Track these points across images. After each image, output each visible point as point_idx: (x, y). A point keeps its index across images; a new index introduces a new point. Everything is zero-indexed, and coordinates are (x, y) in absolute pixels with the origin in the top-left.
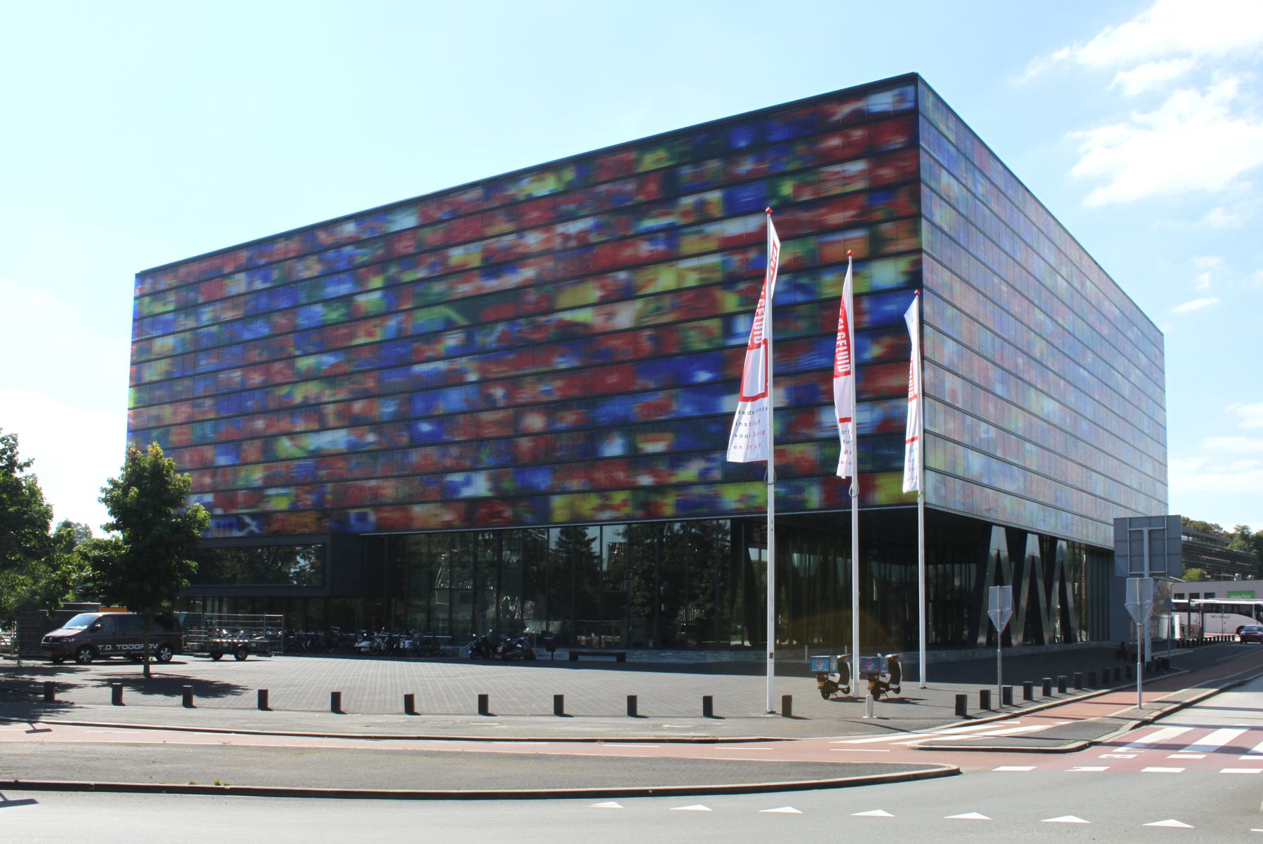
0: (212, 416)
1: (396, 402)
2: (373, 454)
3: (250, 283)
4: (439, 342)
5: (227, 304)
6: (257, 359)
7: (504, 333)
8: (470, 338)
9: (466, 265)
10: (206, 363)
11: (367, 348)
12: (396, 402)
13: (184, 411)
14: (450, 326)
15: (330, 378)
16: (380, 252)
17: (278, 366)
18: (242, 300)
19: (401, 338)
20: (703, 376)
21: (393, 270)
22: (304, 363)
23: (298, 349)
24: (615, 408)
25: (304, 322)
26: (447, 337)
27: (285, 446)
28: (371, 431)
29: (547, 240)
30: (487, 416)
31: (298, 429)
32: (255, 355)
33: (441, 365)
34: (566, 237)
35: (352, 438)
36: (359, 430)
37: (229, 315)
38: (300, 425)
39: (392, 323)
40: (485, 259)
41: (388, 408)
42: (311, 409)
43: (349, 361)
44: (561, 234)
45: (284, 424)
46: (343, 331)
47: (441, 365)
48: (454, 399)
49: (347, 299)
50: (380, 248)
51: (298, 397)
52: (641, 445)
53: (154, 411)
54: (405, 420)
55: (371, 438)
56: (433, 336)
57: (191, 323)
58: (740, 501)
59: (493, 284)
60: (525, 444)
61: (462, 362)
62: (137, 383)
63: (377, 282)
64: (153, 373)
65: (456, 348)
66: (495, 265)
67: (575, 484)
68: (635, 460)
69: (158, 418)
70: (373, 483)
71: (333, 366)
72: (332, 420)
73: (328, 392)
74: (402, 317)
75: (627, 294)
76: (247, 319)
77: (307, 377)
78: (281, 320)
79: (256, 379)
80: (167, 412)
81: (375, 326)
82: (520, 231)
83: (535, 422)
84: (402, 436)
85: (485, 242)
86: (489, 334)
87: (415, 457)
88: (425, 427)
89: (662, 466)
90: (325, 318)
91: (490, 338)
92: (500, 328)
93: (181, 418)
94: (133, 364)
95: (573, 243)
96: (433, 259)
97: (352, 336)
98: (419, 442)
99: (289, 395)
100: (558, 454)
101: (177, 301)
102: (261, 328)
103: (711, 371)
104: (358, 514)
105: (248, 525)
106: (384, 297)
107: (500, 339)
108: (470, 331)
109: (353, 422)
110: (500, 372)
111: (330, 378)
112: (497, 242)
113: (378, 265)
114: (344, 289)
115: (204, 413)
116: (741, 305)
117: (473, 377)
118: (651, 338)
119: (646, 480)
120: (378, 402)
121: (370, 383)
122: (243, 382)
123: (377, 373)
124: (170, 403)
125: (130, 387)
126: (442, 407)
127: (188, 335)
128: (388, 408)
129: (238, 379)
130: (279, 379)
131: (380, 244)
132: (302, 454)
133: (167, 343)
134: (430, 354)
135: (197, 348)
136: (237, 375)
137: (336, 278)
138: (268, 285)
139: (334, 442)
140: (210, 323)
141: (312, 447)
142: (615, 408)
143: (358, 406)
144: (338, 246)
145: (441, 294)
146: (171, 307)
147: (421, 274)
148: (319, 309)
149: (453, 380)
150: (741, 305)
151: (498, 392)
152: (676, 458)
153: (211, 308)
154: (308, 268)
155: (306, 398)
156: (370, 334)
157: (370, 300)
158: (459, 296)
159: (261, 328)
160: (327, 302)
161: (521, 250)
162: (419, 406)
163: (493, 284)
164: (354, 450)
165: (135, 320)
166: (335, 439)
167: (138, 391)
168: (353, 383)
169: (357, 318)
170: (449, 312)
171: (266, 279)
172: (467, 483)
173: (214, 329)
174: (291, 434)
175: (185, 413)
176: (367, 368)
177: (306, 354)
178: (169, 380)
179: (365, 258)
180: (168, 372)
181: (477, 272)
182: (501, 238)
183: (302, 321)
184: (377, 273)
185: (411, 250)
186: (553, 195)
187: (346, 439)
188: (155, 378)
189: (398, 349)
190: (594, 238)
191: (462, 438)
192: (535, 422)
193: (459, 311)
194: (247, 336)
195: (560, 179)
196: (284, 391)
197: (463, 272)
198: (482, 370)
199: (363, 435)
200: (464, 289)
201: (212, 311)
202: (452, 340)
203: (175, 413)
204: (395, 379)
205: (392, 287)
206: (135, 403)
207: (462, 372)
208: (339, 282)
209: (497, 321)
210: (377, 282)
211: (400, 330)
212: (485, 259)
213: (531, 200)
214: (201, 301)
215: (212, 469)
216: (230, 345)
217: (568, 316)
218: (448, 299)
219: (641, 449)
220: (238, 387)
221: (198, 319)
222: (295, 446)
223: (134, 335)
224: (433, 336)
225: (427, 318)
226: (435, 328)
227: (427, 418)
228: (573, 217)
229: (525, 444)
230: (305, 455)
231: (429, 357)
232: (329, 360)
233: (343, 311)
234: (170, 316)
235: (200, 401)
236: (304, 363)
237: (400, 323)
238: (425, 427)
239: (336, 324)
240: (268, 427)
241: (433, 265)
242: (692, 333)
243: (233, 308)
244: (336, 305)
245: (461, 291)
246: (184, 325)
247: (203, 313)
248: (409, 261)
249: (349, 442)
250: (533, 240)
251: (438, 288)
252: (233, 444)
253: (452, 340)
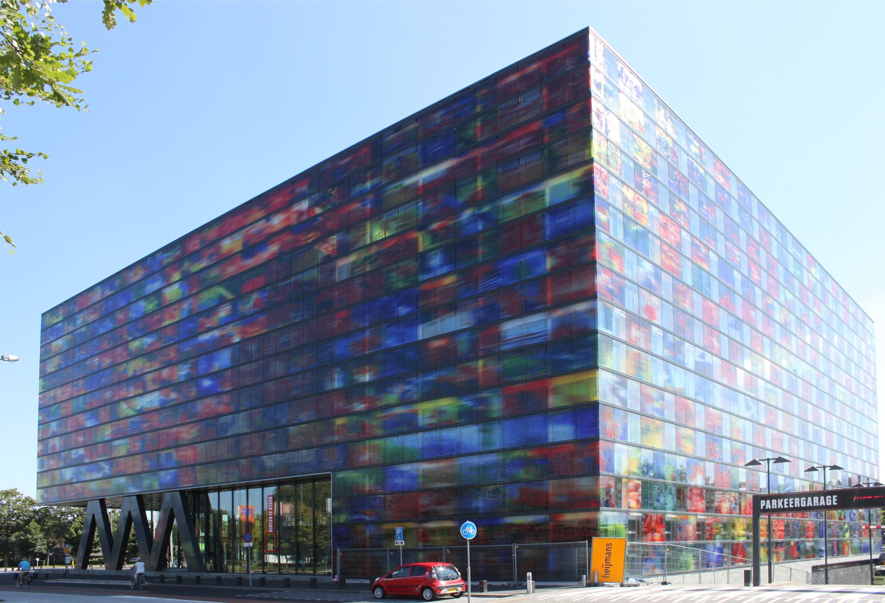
0: (83, 392)
1: (188, 366)
2: (175, 406)
3: (103, 292)
4: (215, 315)
5: (91, 310)
6: (107, 347)
7: (257, 300)
8: (234, 309)
9: (232, 251)
10: (80, 355)
11: (171, 328)
12: (188, 366)
13: (68, 390)
14: (222, 301)
15: (148, 354)
16: (178, 253)
17: (119, 350)
18: (98, 305)
19: (193, 316)
20: (403, 311)
21: (186, 264)
22: (135, 345)
23: (129, 335)
24: (340, 348)
25: (134, 315)
26: (220, 310)
27: (125, 409)
28: (173, 391)
29: (287, 219)
31: (130, 395)
32: (106, 345)
33: (216, 333)
34: (300, 213)
35: (162, 398)
36: (165, 391)
37: (92, 317)
38: (132, 392)
39: (186, 306)
40: (245, 244)
41: (183, 372)
42: (137, 378)
43: (159, 339)
44: (297, 211)
45: (123, 393)
46: (156, 317)
47: (216, 333)
48: (224, 359)
49: (158, 293)
50: (177, 250)
51: (130, 373)
52: (356, 377)
53: (52, 393)
54: (193, 379)
55: (173, 396)
56: (210, 311)
57: (71, 328)
58: (432, 417)
59: (251, 262)
61: (230, 329)
62: (44, 375)
63: (176, 276)
64: (51, 368)
65: (227, 317)
66: (249, 250)
67: (304, 417)
68: (353, 391)
69: (54, 398)
70: (175, 430)
71: (150, 345)
72: (150, 386)
73: (148, 365)
74: (191, 300)
76: (102, 318)
77: (135, 356)
78: (120, 316)
79: (107, 361)
80: (59, 392)
82: (267, 217)
83: (278, 368)
84: (191, 391)
85: (244, 231)
86: (248, 302)
87: (201, 407)
88: (207, 383)
89: (370, 392)
90: (145, 309)
91: (248, 306)
92: (255, 296)
93: (67, 396)
94: (41, 362)
95: (304, 218)
96: (211, 251)
97: (161, 320)
98: (206, 394)
99: (125, 370)
100: (295, 392)
101: (64, 313)
102: (109, 324)
103: (408, 306)
104: (167, 454)
105: (103, 469)
106: (181, 286)
107: (255, 305)
108: (234, 303)
109: (164, 385)
110: (254, 332)
111: (148, 354)
112: (253, 228)
113: (177, 264)
114: (156, 286)
115: (79, 391)
116: (433, 243)
117: (237, 339)
118: (361, 285)
119: (360, 407)
120: (176, 368)
121: (172, 354)
122: (100, 365)
123: (176, 346)
124: (61, 386)
125: (40, 378)
126: (217, 366)
127: (69, 337)
128: (183, 372)
129: (97, 363)
130: (119, 360)
131: (178, 247)
132: (132, 413)
133: (59, 344)
134: (208, 325)
135: (74, 346)
136: (96, 360)
137: (151, 278)
138: (113, 292)
139: (151, 402)
140: (81, 325)
141: (138, 408)
142: (340, 348)
143: (165, 373)
145: (216, 277)
146: (60, 318)
147: (203, 265)
148: (142, 303)
149: (223, 343)
150: (433, 243)
151: (253, 348)
152: (382, 385)
153: (81, 315)
154: (136, 275)
155: (135, 371)
156: (172, 317)
157: (173, 292)
158: (227, 277)
159: (109, 324)
160: (146, 297)
161: (268, 231)
162: (203, 366)
163: (251, 262)
164: (164, 407)
165: (42, 331)
166: (152, 400)
167: (44, 381)
168: (163, 356)
169: (164, 307)
170: (222, 291)
171: (112, 288)
172: (233, 423)
173: (83, 329)
174: (126, 399)
175: (68, 392)
176: (171, 342)
177: (135, 339)
178: (59, 370)
179: (169, 260)
180: (59, 364)
181: (239, 255)
182: (256, 224)
183: (133, 315)
184: (175, 270)
185: (197, 247)
187: (158, 399)
188: (53, 370)
189: (189, 325)
190: (318, 211)
191: (229, 388)
192: (278, 368)
193: (227, 288)
194: (101, 331)
196: (121, 369)
197: (230, 258)
198: (243, 332)
199: (167, 395)
200: (231, 270)
201: (83, 317)
202: (224, 312)
203: (63, 394)
204: (187, 348)
205: (187, 277)
206: (44, 388)
207: (228, 337)
208: (153, 282)
209: (252, 292)
210: (176, 276)
211: (190, 311)
214: (76, 311)
215: (80, 429)
216: (92, 339)
218: (221, 280)
219: (357, 380)
220: (97, 369)
221: (75, 324)
222: (129, 407)
223: (42, 342)
224: (210, 311)
225: (208, 297)
226: (212, 304)
227: (206, 376)
230: (136, 413)
231: (208, 328)
232: (148, 340)
233: (156, 302)
234: (60, 325)
235: (76, 382)
236: (135, 345)
237: (190, 305)
238: (207, 383)
239: (153, 312)
240: (114, 396)
241: (211, 255)
242: (393, 274)
243: (93, 313)
244: (152, 298)
245: (229, 272)
246: (68, 329)
247: (78, 319)
248: (195, 256)
249: (160, 400)
250: (277, 221)
251: (214, 273)
252: (92, 410)
253: (224, 312)
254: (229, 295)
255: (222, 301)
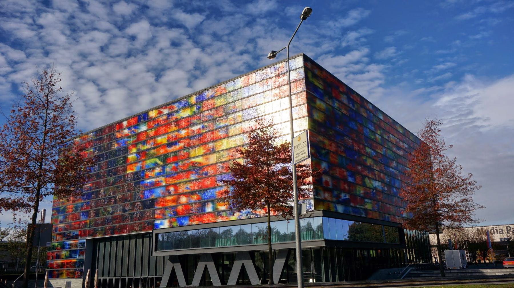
9: (162, 143)
24: (209, 193)
29: (187, 133)
30: (169, 198)
33: (154, 180)
34: (194, 131)
39: (139, 165)
60: (181, 208)
75: (213, 151)
81: (133, 166)
108: (163, 167)
144: (122, 138)
149: (157, 184)
151: (172, 189)
156: (132, 169)
170: (157, 160)
186: (190, 117)
192: (184, 199)
195: (191, 110)
200: (162, 151)
202: (158, 170)
212: (168, 140)
213: (182, 118)
217: (194, 160)
224: (151, 169)
226: (152, 166)
228: (195, 124)
229: (181, 208)
248: (144, 143)
250: (183, 133)
253: (158, 170)
254: (161, 163)
255: (157, 165)
